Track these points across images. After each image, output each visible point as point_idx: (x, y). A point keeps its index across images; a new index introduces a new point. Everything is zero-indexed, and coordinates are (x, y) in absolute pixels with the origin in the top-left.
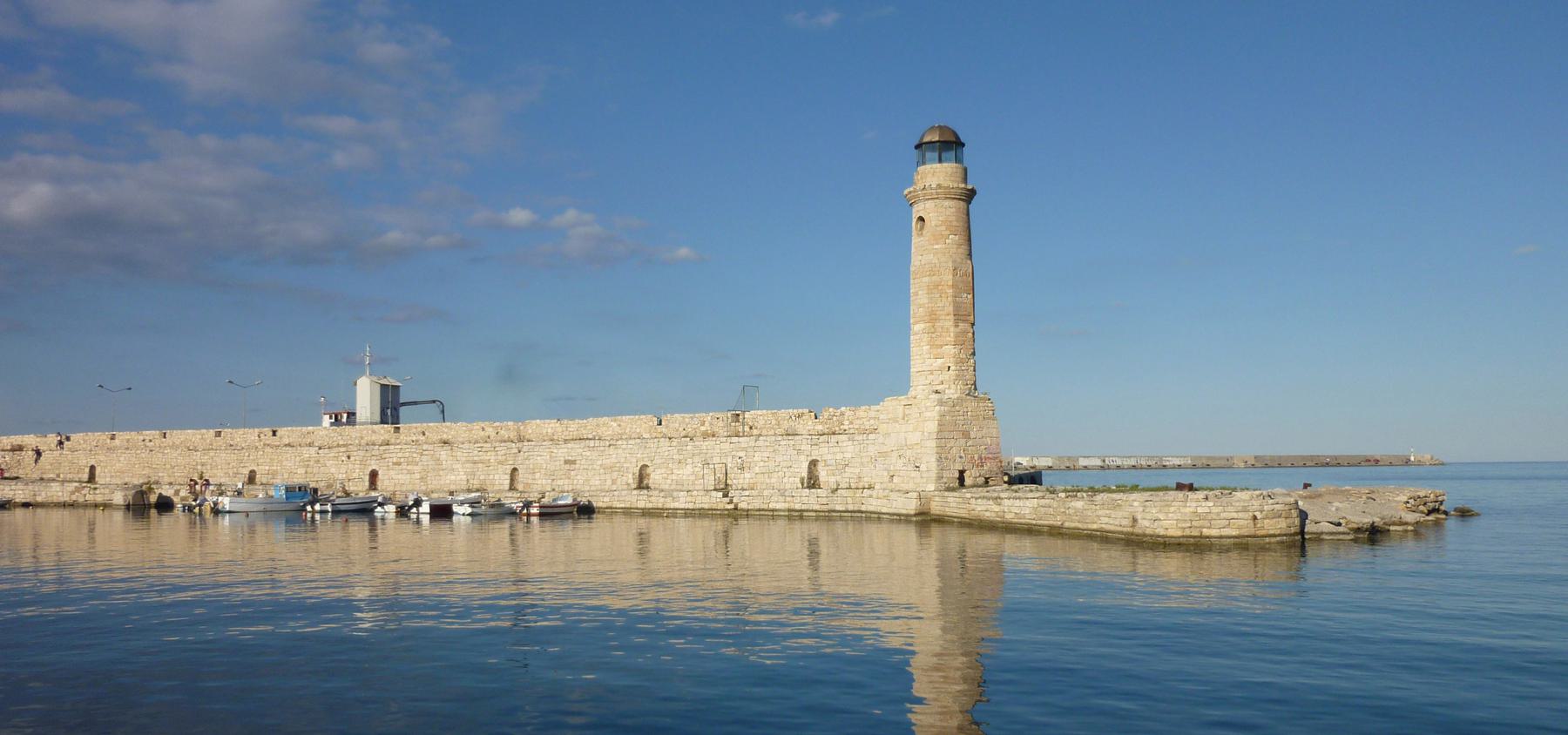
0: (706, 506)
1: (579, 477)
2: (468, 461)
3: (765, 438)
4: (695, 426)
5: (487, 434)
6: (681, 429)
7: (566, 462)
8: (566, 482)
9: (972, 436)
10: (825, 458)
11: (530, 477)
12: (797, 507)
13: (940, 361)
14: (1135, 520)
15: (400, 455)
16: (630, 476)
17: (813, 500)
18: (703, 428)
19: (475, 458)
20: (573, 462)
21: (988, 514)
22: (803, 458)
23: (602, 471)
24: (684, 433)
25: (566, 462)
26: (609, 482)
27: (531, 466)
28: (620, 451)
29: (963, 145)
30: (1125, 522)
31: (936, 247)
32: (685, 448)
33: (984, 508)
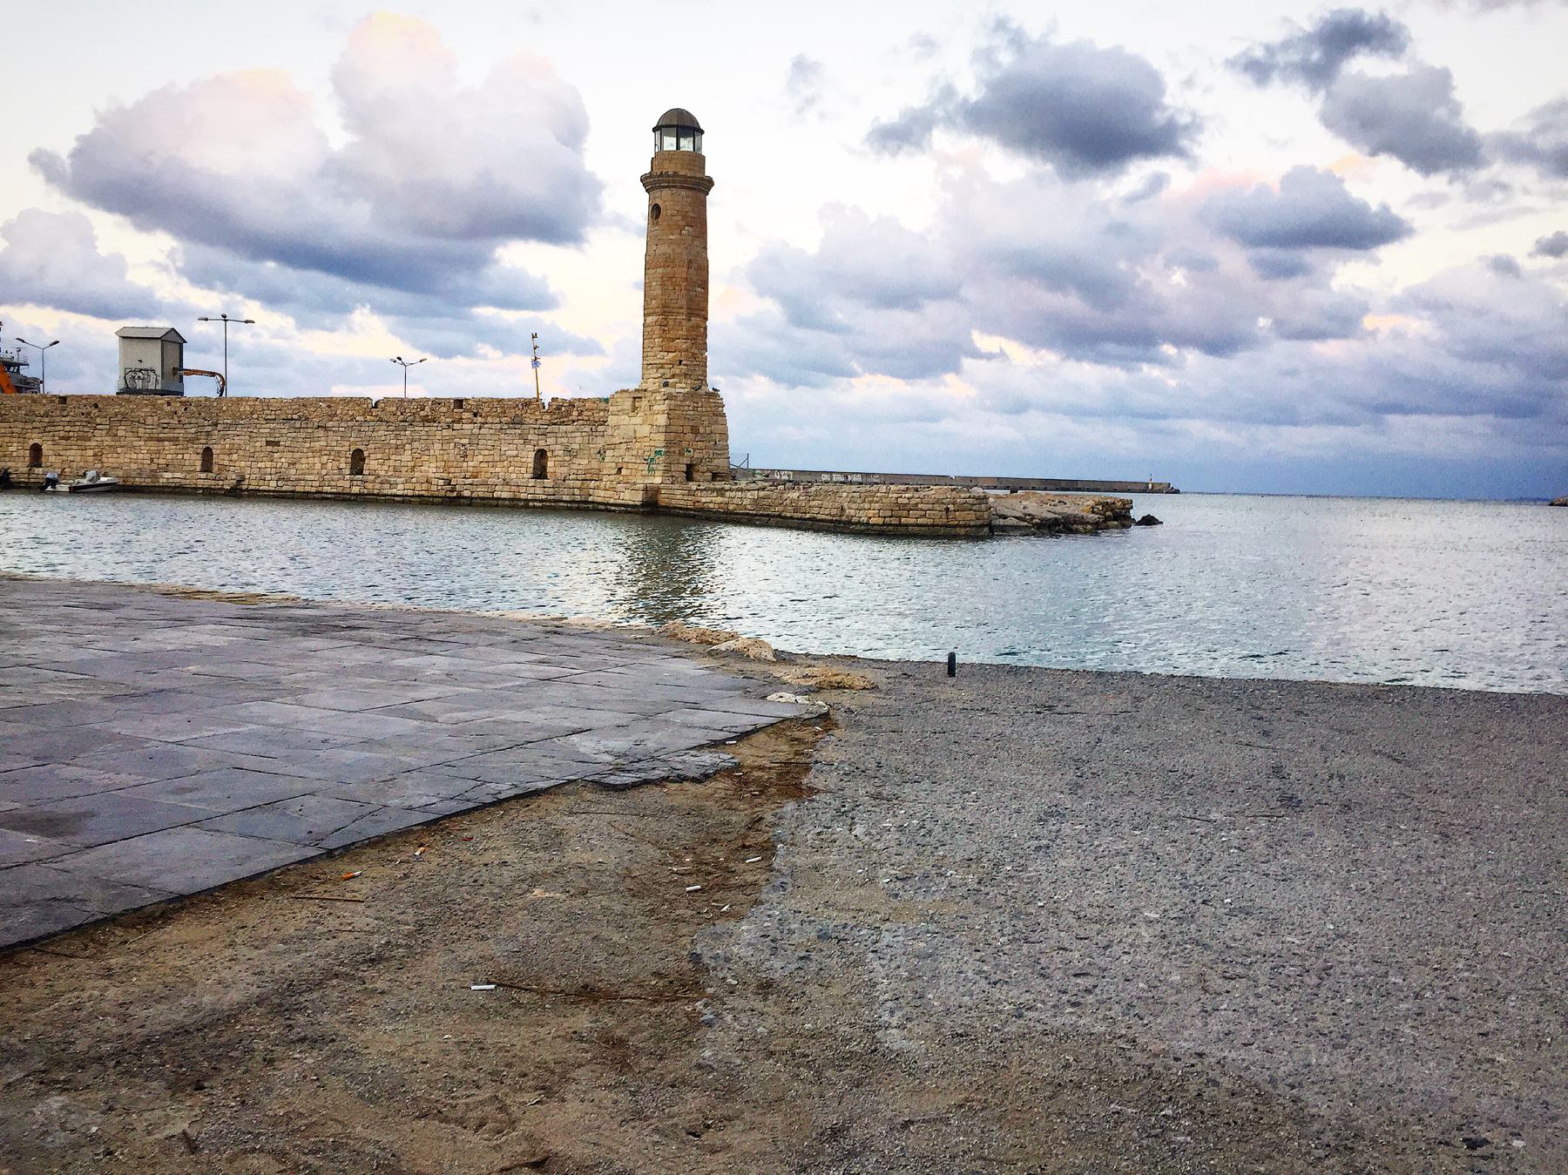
1: (283, 460)
2: (150, 439)
3: (489, 426)
4: (414, 411)
6: (399, 413)
7: (268, 443)
8: (269, 464)
9: (701, 430)
10: (552, 448)
11: (227, 457)
12: (523, 496)
13: (671, 355)
14: (842, 509)
15: (68, 428)
17: (539, 491)
18: (422, 413)
19: (160, 435)
20: (277, 444)
21: (711, 506)
22: (530, 447)
23: (310, 454)
25: (268, 443)
26: (318, 466)
27: (227, 446)
28: (330, 433)
29: (702, 132)
30: (834, 512)
31: (671, 237)
32: (402, 433)
33: (708, 500)
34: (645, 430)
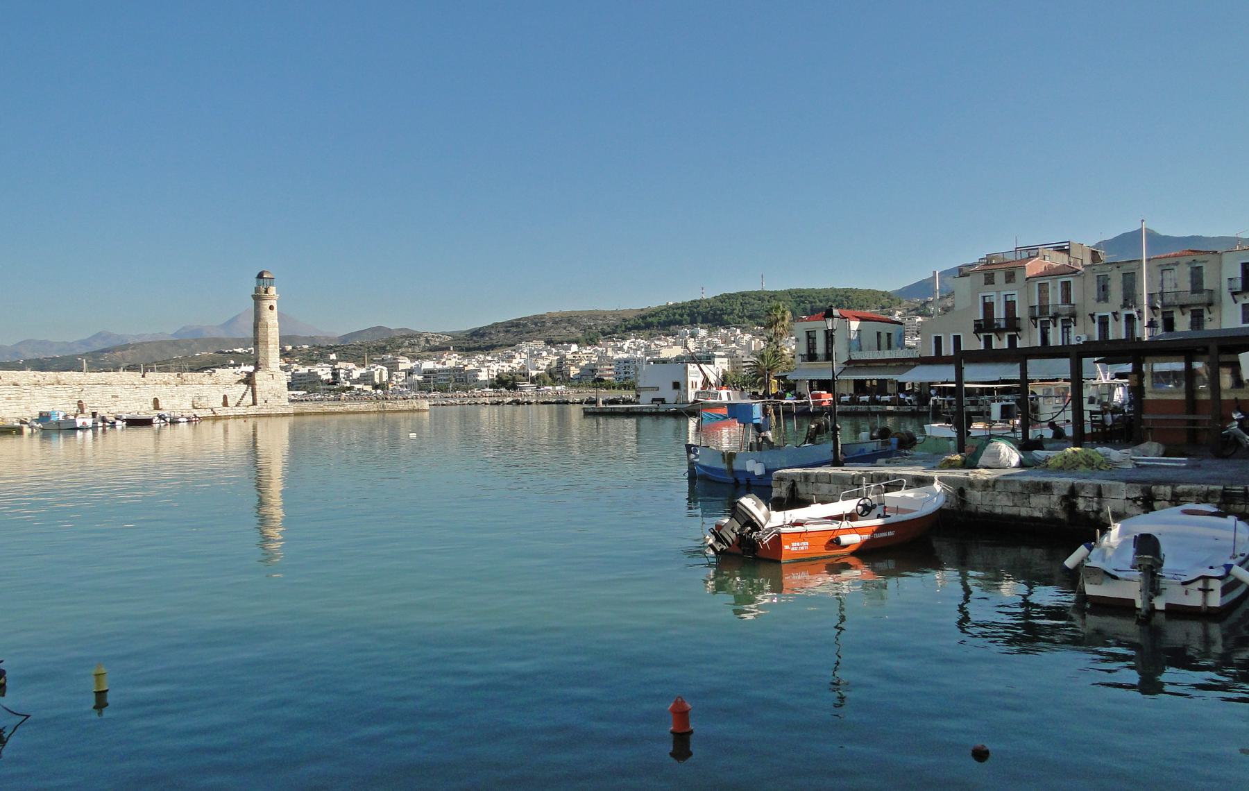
0: (206, 416)
5: (37, 379)
7: (113, 396)
15: (9, 392)
16: (150, 403)
18: (164, 380)
20: (117, 397)
23: (134, 401)
24: (155, 382)
25: (113, 396)
26: (139, 407)
34: (277, 386)
